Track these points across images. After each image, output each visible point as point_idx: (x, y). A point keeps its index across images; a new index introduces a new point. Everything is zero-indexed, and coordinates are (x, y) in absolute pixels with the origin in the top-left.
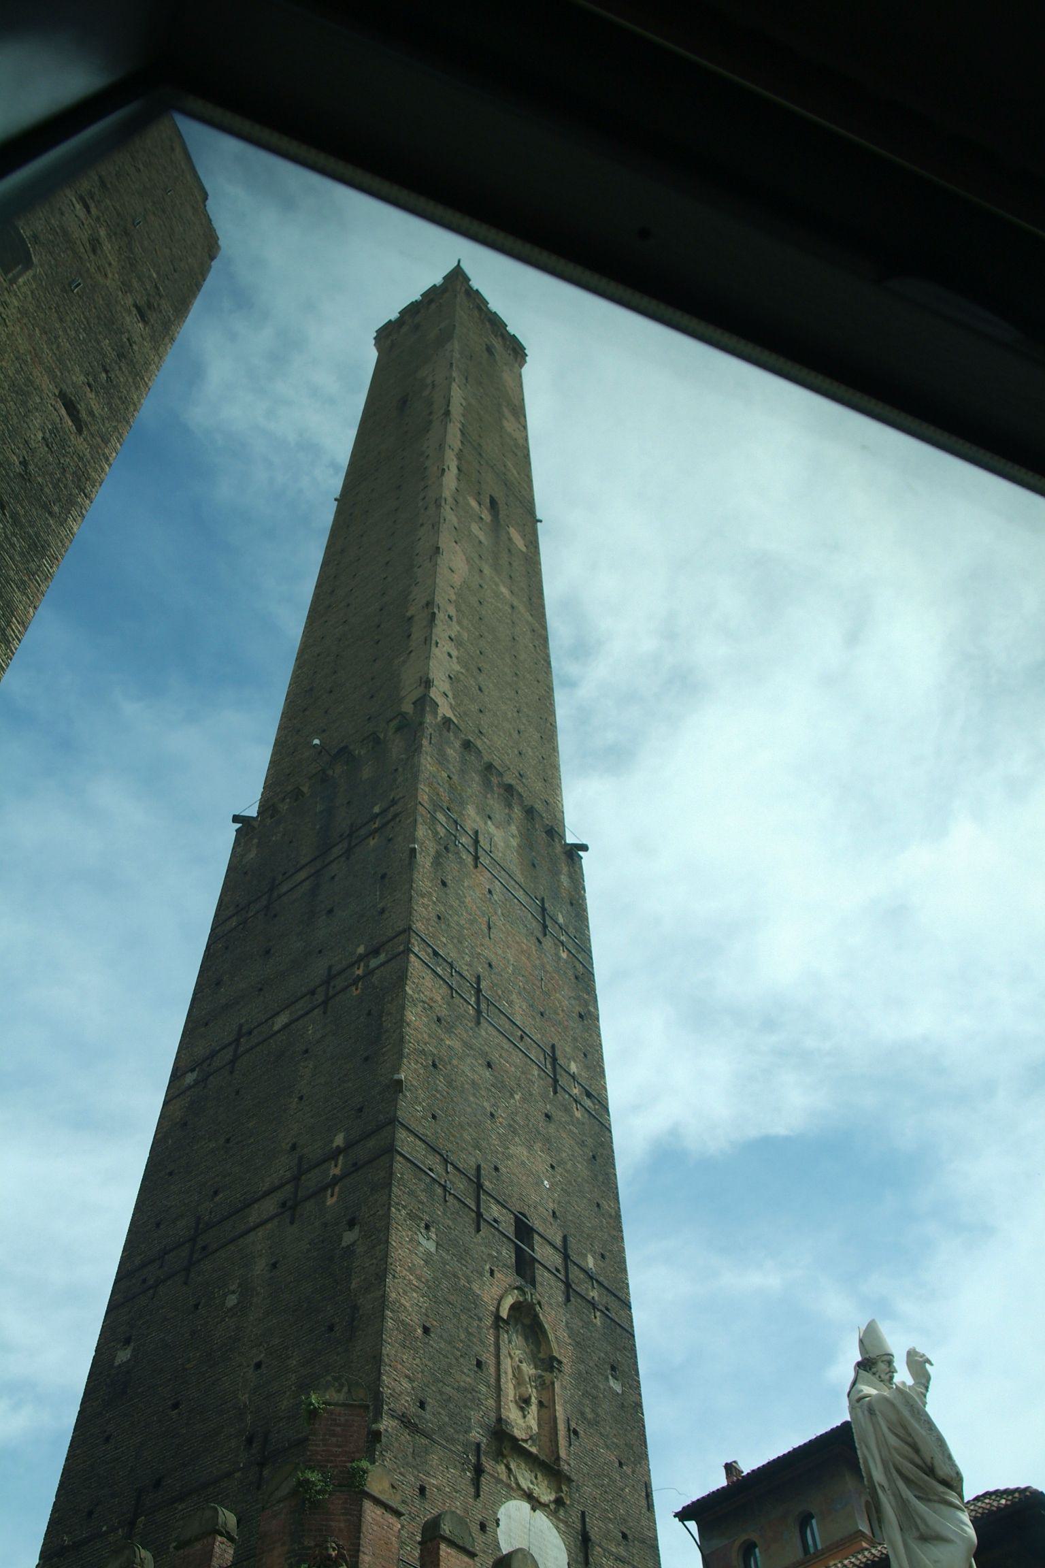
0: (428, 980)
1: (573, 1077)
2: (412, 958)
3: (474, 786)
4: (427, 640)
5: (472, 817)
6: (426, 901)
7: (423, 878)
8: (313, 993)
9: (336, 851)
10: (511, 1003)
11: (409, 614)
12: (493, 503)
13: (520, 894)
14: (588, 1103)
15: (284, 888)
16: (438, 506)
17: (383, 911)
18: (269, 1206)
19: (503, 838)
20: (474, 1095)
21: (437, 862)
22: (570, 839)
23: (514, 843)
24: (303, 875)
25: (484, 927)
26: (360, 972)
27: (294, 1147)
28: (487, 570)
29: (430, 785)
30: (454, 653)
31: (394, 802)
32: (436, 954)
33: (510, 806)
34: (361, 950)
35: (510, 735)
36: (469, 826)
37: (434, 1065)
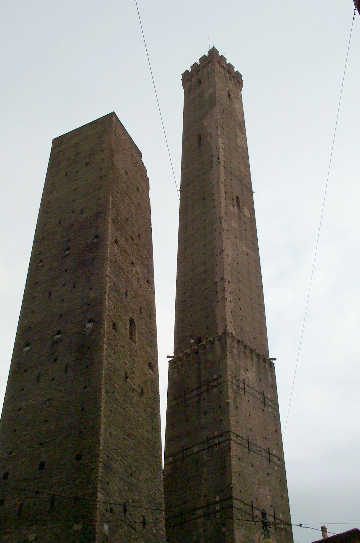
1: (275, 455)
2: (232, 442)
4: (223, 298)
7: (232, 410)
8: (204, 443)
9: (204, 388)
10: (256, 440)
11: (216, 280)
13: (258, 396)
14: (278, 462)
15: (189, 396)
16: (221, 222)
17: (221, 420)
18: (200, 512)
19: (250, 376)
21: (235, 401)
22: (270, 357)
24: (194, 393)
26: (217, 441)
27: (205, 496)
30: (232, 299)
31: (220, 376)
33: (252, 359)
34: (216, 433)
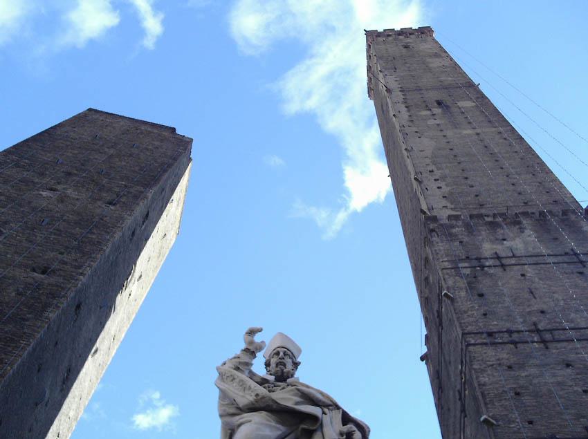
0: (490, 352)
3: (484, 232)
5: (488, 248)
6: (470, 313)
12: (439, 103)
13: (551, 260)
20: (562, 389)
21: (471, 286)
23: (533, 238)
25: (527, 295)
28: (449, 133)
29: (447, 256)
32: (490, 334)
35: (507, 190)
36: (487, 254)
37: (517, 394)
